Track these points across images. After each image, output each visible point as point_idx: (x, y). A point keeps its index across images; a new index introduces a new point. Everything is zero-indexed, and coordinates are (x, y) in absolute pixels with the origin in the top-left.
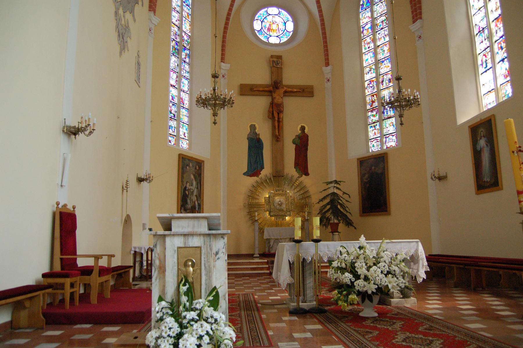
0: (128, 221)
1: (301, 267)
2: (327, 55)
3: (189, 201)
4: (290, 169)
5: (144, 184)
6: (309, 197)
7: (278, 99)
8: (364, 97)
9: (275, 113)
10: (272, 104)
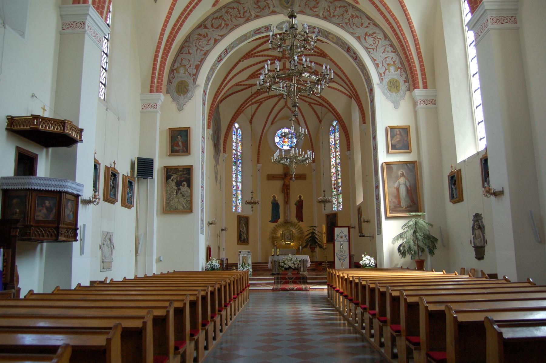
0: (219, 248)
1: (274, 262)
3: (243, 239)
4: (294, 219)
5: (224, 232)
7: (287, 183)
8: (331, 181)
9: (286, 189)
10: (284, 185)
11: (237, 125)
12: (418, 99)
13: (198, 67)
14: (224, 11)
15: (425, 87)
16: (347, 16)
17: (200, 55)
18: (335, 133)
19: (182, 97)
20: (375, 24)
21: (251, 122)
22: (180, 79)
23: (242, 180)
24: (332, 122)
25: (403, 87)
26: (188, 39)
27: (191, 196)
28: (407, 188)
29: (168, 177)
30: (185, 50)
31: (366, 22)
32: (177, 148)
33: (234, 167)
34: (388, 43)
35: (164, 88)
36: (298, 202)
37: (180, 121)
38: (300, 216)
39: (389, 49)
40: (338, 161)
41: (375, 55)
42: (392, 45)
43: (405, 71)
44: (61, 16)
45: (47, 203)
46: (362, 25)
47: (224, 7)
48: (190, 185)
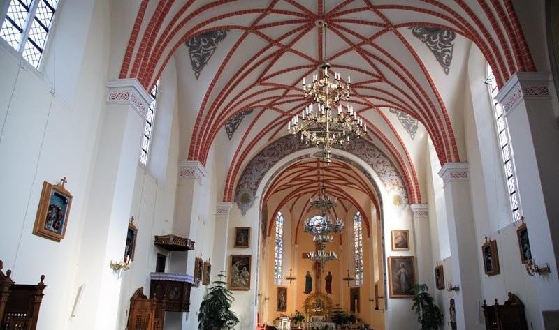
2: (341, 242)
4: (324, 291)
6: (331, 303)
11: (279, 213)
12: (414, 211)
13: (257, 184)
14: (276, 144)
15: (420, 202)
16: (364, 149)
17: (258, 177)
18: (358, 221)
19: (245, 205)
20: (384, 155)
21: (291, 210)
22: (244, 192)
23: (282, 257)
24: (356, 212)
25: (404, 201)
26: (250, 164)
27: (249, 277)
28: (406, 277)
29: (233, 263)
30: (248, 171)
31: (378, 154)
32: (240, 242)
33: (276, 247)
34: (393, 169)
35: (233, 198)
36: (327, 276)
37: (244, 224)
38: (329, 289)
39: (394, 173)
40: (361, 245)
41: (383, 177)
42: (396, 171)
43: (406, 190)
44: (180, 167)
45: (176, 289)
46: (374, 155)
47: (277, 141)
48: (249, 270)
